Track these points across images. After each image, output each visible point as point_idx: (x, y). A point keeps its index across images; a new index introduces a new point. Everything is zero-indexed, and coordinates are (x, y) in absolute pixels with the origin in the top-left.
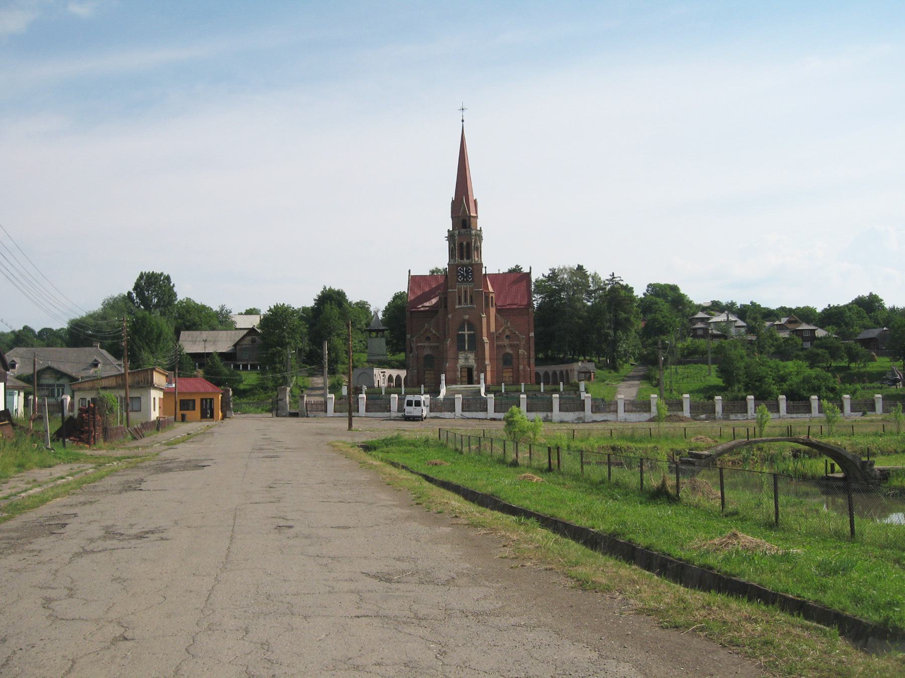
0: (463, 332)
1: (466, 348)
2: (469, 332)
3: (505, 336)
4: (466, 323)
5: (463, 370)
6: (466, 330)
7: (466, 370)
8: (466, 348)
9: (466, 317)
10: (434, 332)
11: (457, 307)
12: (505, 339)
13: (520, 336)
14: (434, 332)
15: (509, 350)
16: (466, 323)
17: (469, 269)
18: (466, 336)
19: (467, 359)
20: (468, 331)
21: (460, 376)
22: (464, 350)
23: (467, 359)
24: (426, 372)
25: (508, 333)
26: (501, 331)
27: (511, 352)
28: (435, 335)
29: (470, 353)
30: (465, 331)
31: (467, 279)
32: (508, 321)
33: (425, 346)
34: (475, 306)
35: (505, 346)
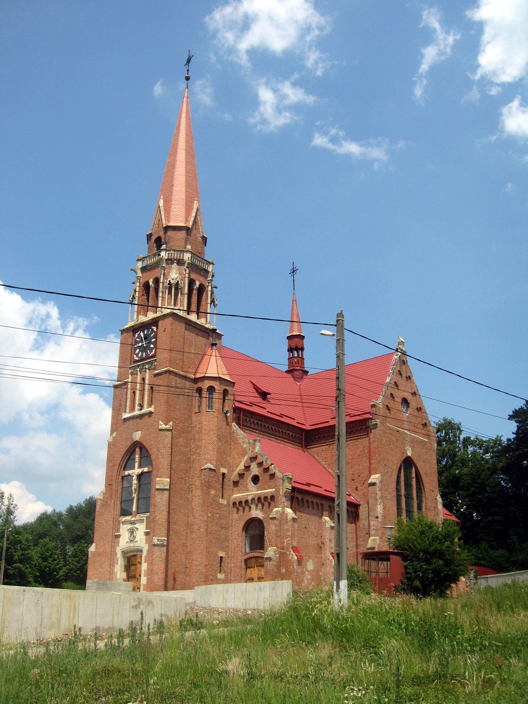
1: (134, 509)
3: (249, 479)
4: (138, 450)
6: (137, 465)
8: (134, 509)
9: (137, 436)
12: (251, 485)
13: (279, 475)
15: (256, 513)
16: (138, 450)
17: (153, 331)
18: (135, 478)
19: (132, 533)
20: (140, 467)
22: (130, 514)
23: (132, 532)
25: (255, 470)
26: (241, 467)
30: (134, 468)
31: (147, 354)
32: (255, 441)
35: (247, 501)
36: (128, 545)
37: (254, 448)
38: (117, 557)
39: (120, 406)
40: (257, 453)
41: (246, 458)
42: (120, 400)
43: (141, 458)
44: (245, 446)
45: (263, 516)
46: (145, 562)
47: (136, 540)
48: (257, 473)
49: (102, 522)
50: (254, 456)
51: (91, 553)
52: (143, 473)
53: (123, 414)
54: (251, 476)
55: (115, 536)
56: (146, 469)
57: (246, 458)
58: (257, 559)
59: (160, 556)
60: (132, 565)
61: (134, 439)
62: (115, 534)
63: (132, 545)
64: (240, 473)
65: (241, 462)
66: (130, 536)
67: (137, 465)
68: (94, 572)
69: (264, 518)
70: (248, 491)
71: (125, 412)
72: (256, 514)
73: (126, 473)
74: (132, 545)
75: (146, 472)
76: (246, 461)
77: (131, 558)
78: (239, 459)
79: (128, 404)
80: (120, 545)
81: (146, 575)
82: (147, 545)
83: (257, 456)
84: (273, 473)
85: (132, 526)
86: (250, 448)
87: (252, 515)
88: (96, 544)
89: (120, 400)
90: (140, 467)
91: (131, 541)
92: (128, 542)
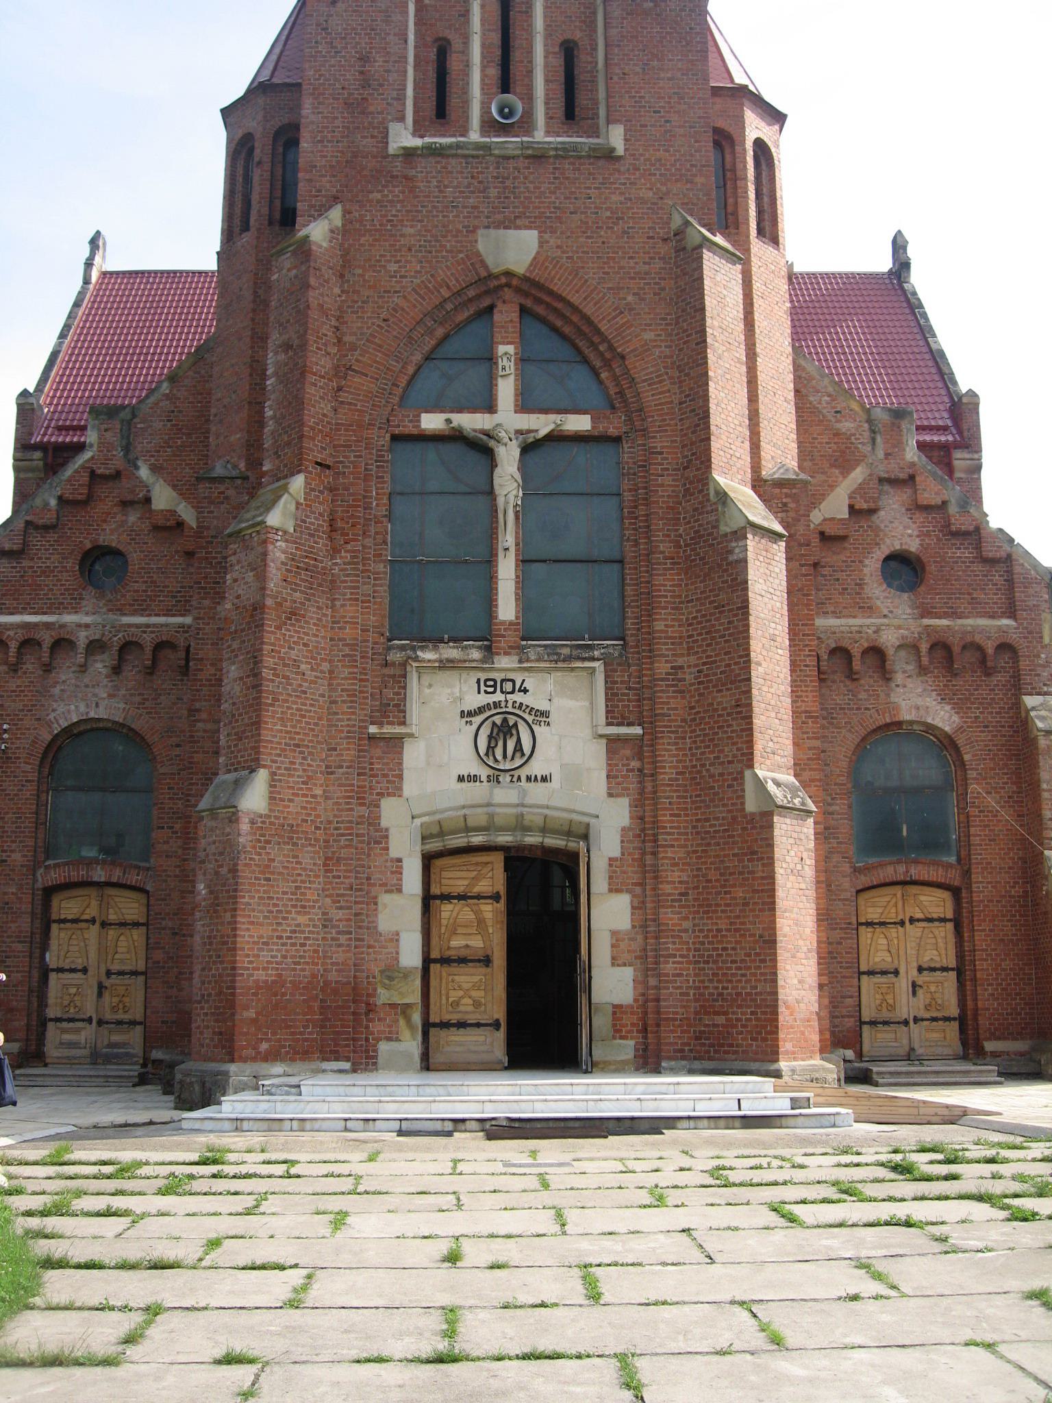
0: (470, 422)
1: (507, 609)
2: (542, 424)
3: (872, 565)
4: (506, 315)
5: (454, 878)
6: (506, 390)
7: (493, 877)
10: (163, 497)
11: (403, 137)
12: (877, 590)
14: (163, 497)
19: (504, 730)
20: (524, 405)
21: (410, 954)
23: (504, 730)
24: (66, 906)
27: (943, 718)
28: (172, 527)
29: (558, 660)
30: (491, 408)
33: (62, 644)
34: (616, 138)
35: (876, 653)
36: (477, 792)
37: (899, 444)
38: (394, 853)
39: (366, 84)
40: (913, 464)
41: (858, 475)
42: (364, 59)
43: (523, 360)
44: (846, 426)
45: (956, 718)
46: (614, 889)
47: (537, 767)
48: (913, 546)
49: (293, 654)
50: (902, 476)
51: (252, 822)
52: (556, 438)
53: (394, 128)
54: (880, 553)
55: (372, 738)
56: (580, 423)
57: (858, 475)
58: (914, 889)
59: (799, 867)
60: (446, 897)
61: (490, 261)
62: (373, 729)
63: (505, 795)
64: (830, 530)
65: (832, 487)
66: (490, 749)
67: (506, 390)
68: (266, 931)
69: (960, 729)
70: (868, 609)
71: (402, 119)
72: (918, 708)
73: (432, 422)
74: (505, 795)
75: (579, 438)
76: (860, 490)
77: (438, 863)
78: (820, 477)
79: (410, 92)
80: (409, 788)
81: (626, 956)
82: (624, 802)
83: (912, 478)
84: (1004, 554)
85: (499, 697)
86: (874, 440)
87: (897, 708)
88: (273, 774)
89: (364, 59)
90: (524, 405)
91: (494, 779)
92: (474, 778)
